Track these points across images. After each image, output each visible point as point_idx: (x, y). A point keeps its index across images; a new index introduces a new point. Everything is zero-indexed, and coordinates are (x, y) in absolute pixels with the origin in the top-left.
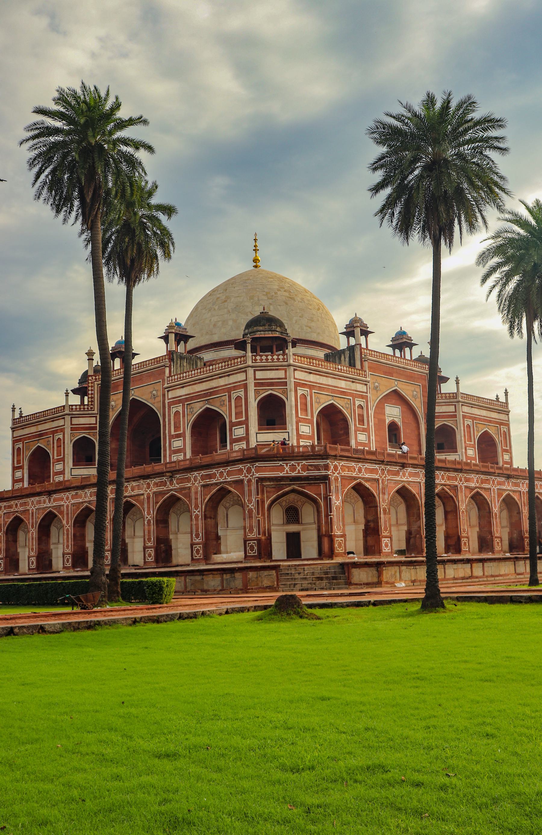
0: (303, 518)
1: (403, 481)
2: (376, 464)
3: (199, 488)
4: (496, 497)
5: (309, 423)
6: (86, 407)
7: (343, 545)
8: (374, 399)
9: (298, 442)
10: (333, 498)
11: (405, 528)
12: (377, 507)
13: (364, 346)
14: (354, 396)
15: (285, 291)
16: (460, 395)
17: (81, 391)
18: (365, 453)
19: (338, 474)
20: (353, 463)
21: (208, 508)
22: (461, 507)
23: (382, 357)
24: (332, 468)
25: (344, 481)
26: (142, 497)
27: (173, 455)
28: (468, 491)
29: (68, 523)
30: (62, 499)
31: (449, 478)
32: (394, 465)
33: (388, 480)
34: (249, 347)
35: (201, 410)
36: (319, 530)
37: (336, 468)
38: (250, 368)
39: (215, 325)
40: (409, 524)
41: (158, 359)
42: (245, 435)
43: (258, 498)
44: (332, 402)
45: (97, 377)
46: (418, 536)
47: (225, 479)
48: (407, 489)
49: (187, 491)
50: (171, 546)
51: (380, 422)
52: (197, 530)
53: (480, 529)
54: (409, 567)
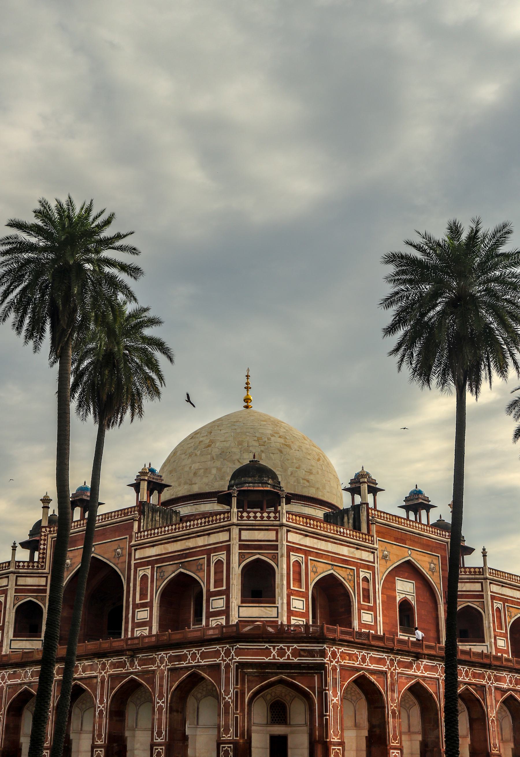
0: (291, 717)
1: (417, 676)
2: (383, 652)
3: (166, 673)
5: (303, 597)
6: (35, 564)
8: (382, 570)
9: (289, 620)
11: (420, 738)
12: (384, 707)
13: (371, 505)
14: (359, 566)
15: (280, 437)
16: (488, 571)
17: (32, 545)
18: (371, 638)
19: (337, 662)
20: (356, 650)
23: (393, 520)
25: (344, 672)
26: (95, 681)
27: (136, 629)
28: (499, 694)
31: (474, 675)
32: (406, 655)
33: (398, 673)
34: (234, 501)
35: (173, 575)
37: (334, 655)
38: (235, 527)
39: (195, 474)
40: (424, 733)
41: (126, 511)
42: (224, 608)
43: (237, 688)
44: (332, 571)
45: (52, 529)
46: (435, 749)
47: (198, 662)
49: (151, 675)
50: (125, 747)
51: (389, 599)
52: (160, 727)
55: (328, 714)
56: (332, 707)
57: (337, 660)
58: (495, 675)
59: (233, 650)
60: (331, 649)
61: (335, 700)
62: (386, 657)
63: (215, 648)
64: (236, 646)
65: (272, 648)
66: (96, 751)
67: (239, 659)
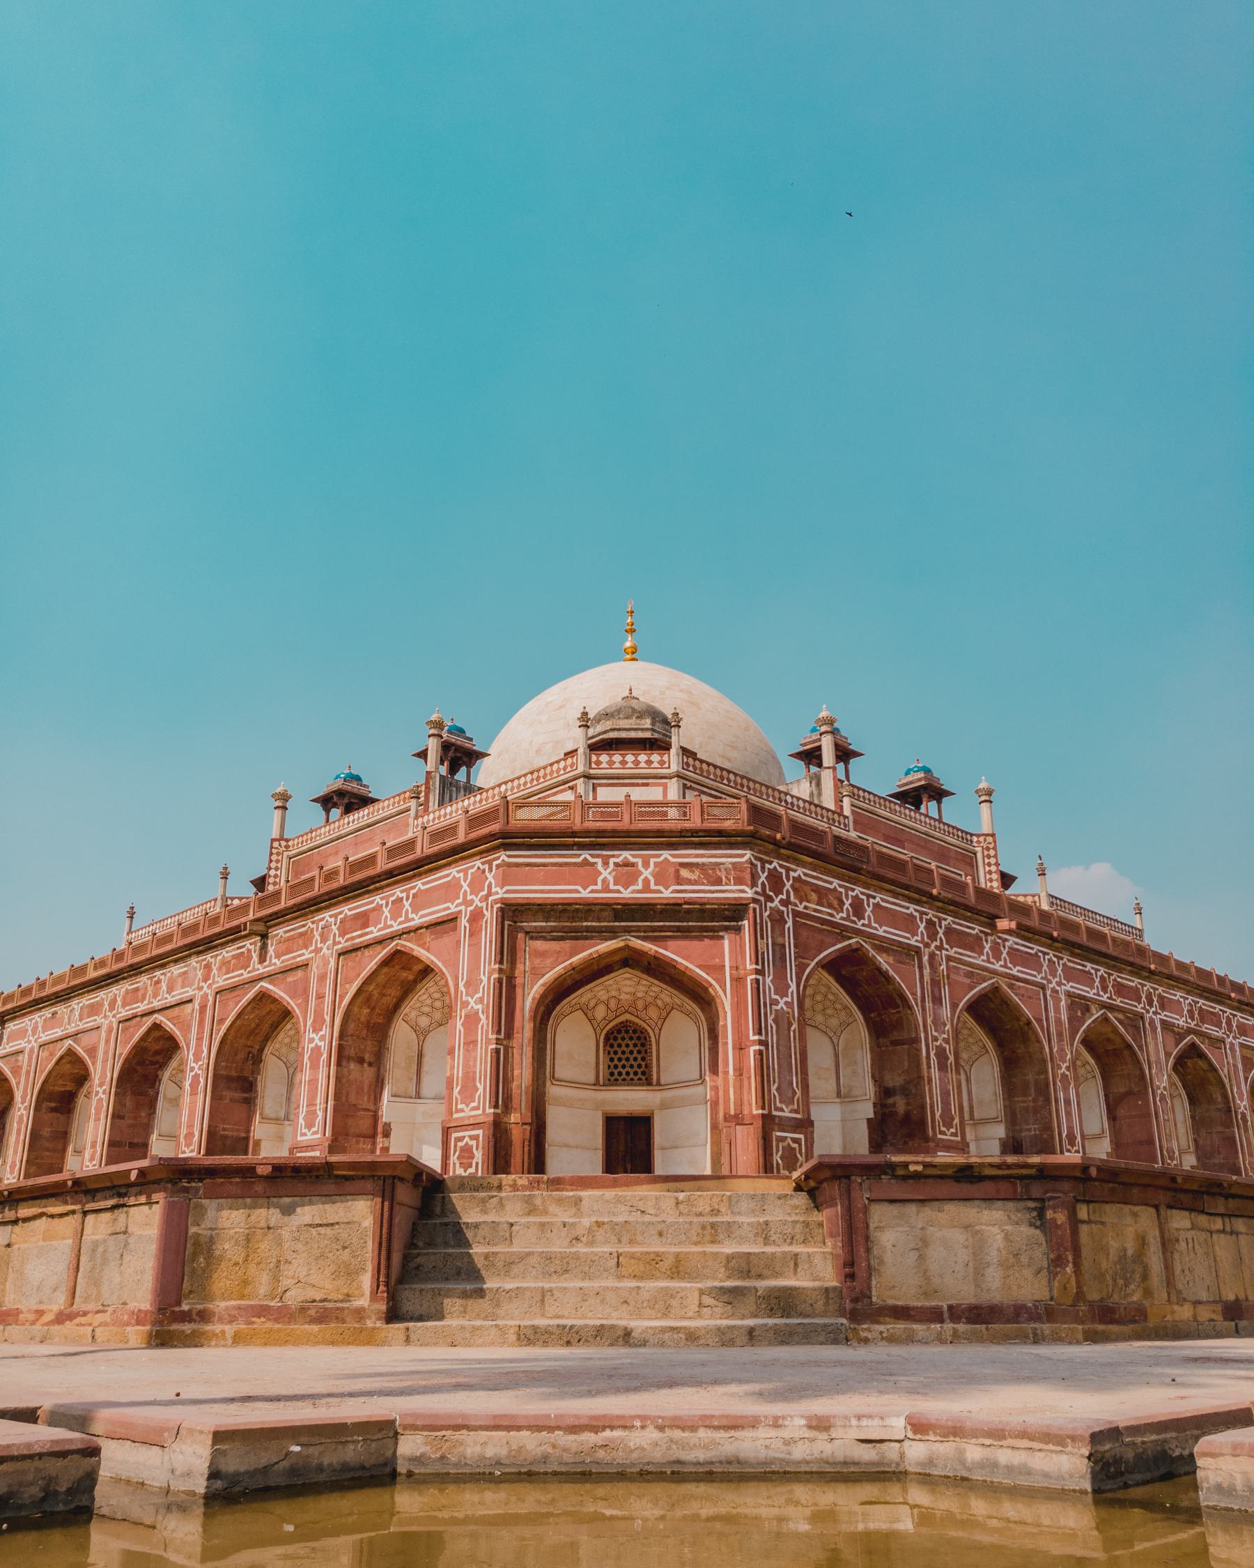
4: (1240, 1066)
11: (1000, 1131)
12: (917, 1040)
18: (873, 859)
20: (836, 882)
24: (763, 877)
25: (804, 933)
26: (189, 1006)
28: (1171, 1040)
30: (22, 1034)
31: (1121, 989)
33: (949, 958)
37: (776, 881)
39: (538, 751)
40: (1012, 1118)
45: (290, 843)
47: (407, 920)
48: (1006, 1003)
53: (1198, 1159)
54: (1202, 1220)
55: (763, 1038)
56: (775, 1020)
57: (784, 897)
58: (1161, 998)
59: (490, 870)
60: (767, 866)
61: (782, 1004)
62: (916, 914)
63: (448, 875)
64: (498, 858)
65: (599, 861)
67: (507, 892)
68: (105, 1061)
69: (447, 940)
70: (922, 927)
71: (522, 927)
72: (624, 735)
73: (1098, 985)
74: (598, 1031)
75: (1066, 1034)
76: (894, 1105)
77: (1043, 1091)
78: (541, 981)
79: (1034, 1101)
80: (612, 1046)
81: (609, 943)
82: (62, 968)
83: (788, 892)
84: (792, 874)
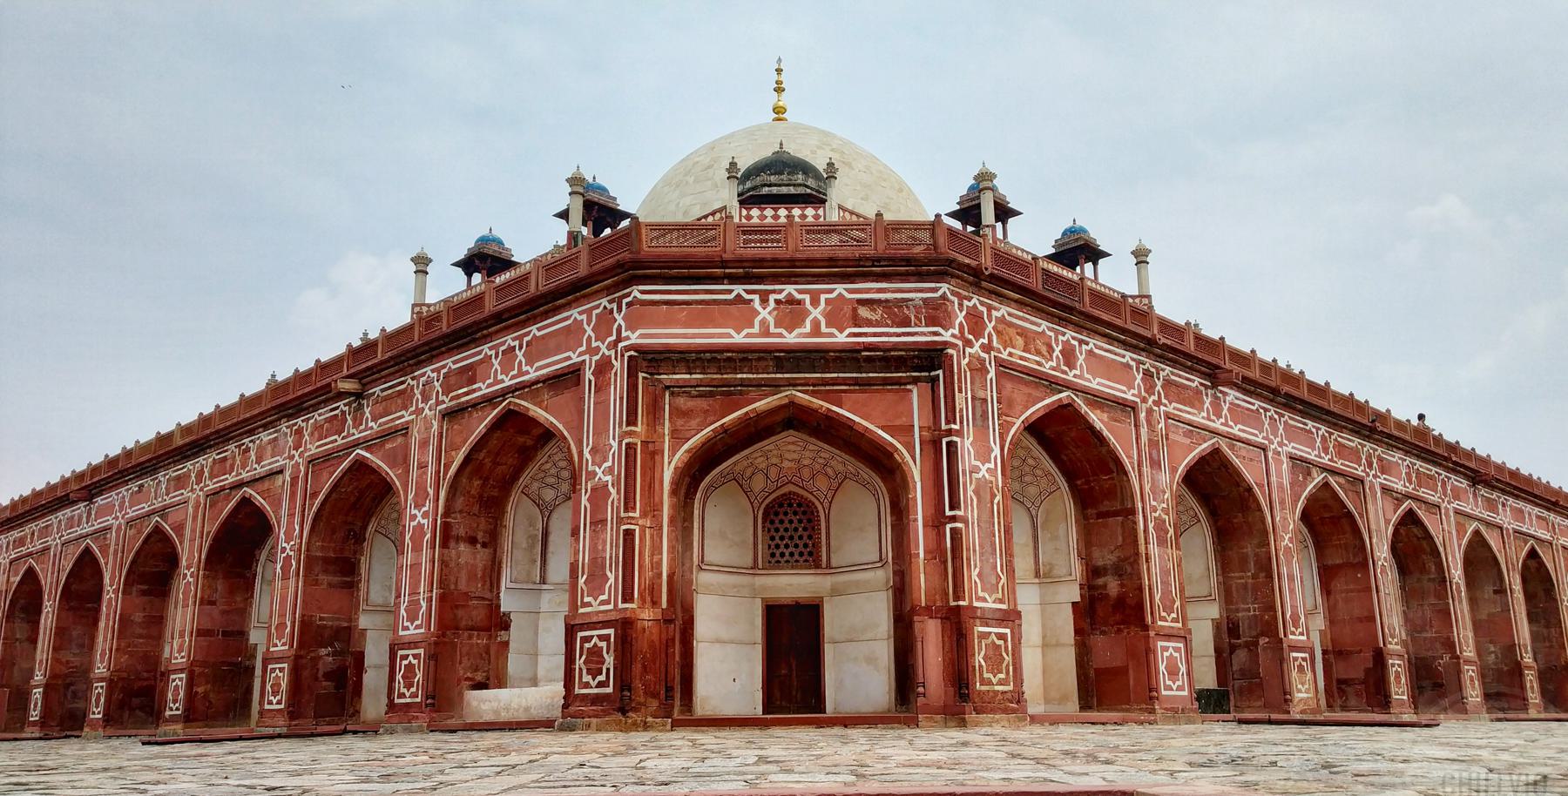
3: (435, 424)
7: (1008, 659)
10: (966, 445)
11: (1214, 611)
12: (1133, 512)
18: (1087, 299)
21: (460, 502)
22: (1377, 554)
24: (961, 317)
25: (1009, 386)
26: (279, 480)
28: (1390, 506)
29: (112, 579)
30: (108, 510)
31: (1341, 450)
33: (1168, 416)
36: (901, 590)
37: (975, 323)
46: (1263, 641)
56: (976, 492)
57: (986, 341)
60: (966, 303)
61: (983, 471)
62: (1133, 364)
64: (628, 295)
66: (273, 670)
68: (192, 540)
69: (566, 397)
70: (1139, 377)
71: (660, 381)
72: (775, 190)
73: (1318, 444)
74: (756, 504)
75: (1288, 500)
76: (1105, 586)
77: (1265, 567)
78: (686, 447)
79: (1254, 577)
80: (772, 522)
81: (769, 399)
82: (147, 436)
83: (990, 335)
84: (994, 313)
